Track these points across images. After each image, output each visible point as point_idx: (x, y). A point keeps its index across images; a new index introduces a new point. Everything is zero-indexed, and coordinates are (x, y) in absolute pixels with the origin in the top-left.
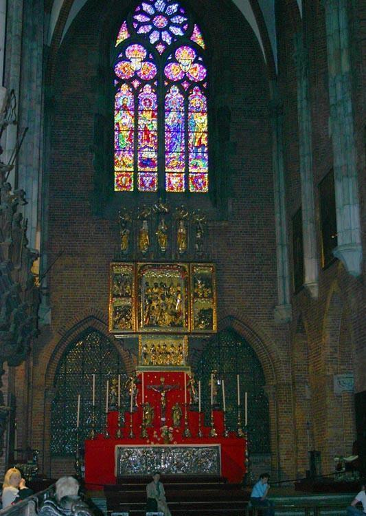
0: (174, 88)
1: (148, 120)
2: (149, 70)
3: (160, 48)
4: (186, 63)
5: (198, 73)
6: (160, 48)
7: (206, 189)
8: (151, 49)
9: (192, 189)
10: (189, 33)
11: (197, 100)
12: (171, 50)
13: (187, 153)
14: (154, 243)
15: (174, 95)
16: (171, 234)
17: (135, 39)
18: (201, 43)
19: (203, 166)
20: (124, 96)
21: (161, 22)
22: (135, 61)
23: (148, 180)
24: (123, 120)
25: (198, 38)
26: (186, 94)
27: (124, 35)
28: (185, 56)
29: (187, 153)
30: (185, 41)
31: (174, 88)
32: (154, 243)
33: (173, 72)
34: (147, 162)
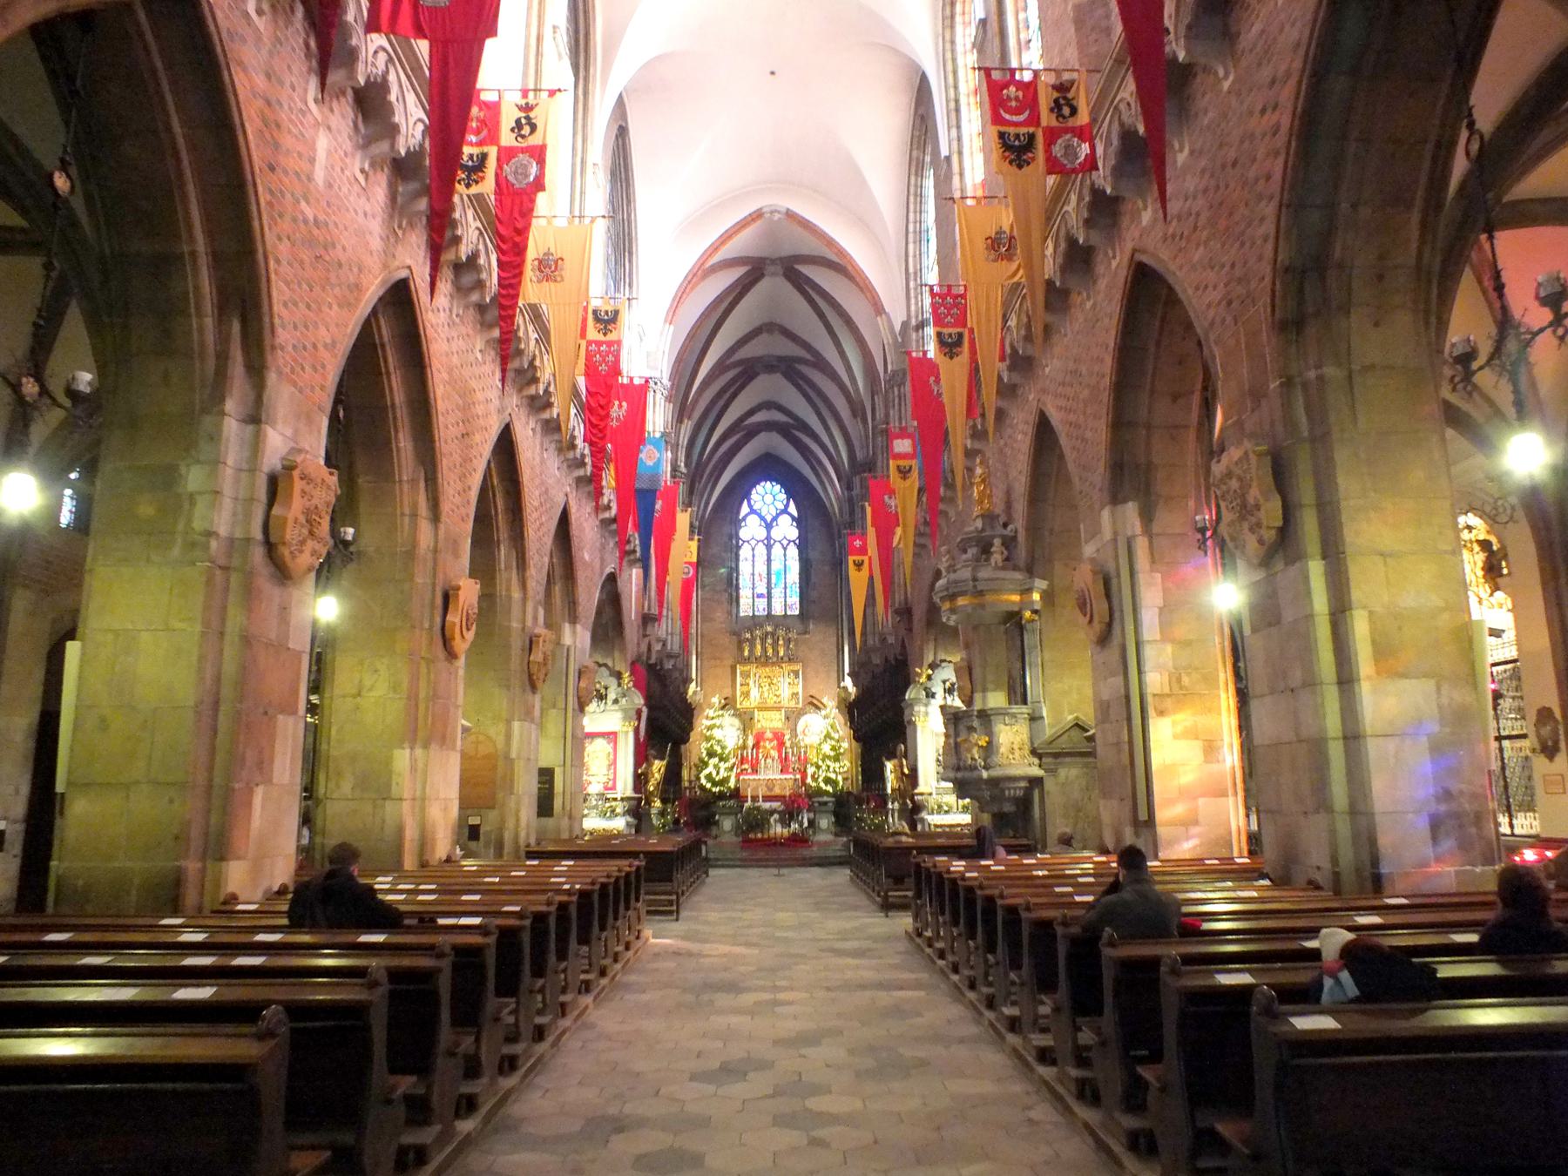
0: (777, 544)
1: (761, 568)
2: (763, 533)
3: (769, 519)
4: (787, 529)
5: (793, 533)
6: (769, 519)
7: (797, 612)
8: (762, 518)
9: (789, 613)
10: (787, 506)
11: (793, 552)
12: (775, 519)
13: (785, 588)
14: (764, 649)
15: (777, 551)
16: (775, 644)
17: (753, 511)
18: (795, 514)
19: (794, 599)
20: (745, 552)
21: (769, 498)
22: (751, 529)
23: (761, 609)
24: (745, 568)
25: (793, 509)
26: (785, 549)
27: (745, 509)
28: (785, 520)
29: (785, 588)
30: (785, 511)
31: (777, 544)
32: (764, 649)
33: (776, 533)
34: (760, 596)
